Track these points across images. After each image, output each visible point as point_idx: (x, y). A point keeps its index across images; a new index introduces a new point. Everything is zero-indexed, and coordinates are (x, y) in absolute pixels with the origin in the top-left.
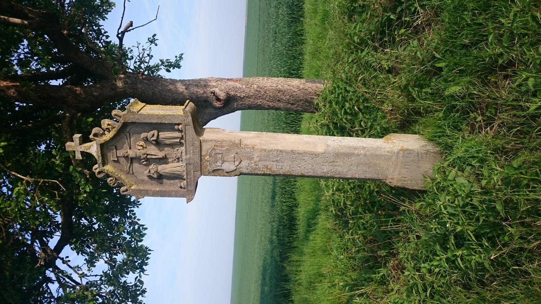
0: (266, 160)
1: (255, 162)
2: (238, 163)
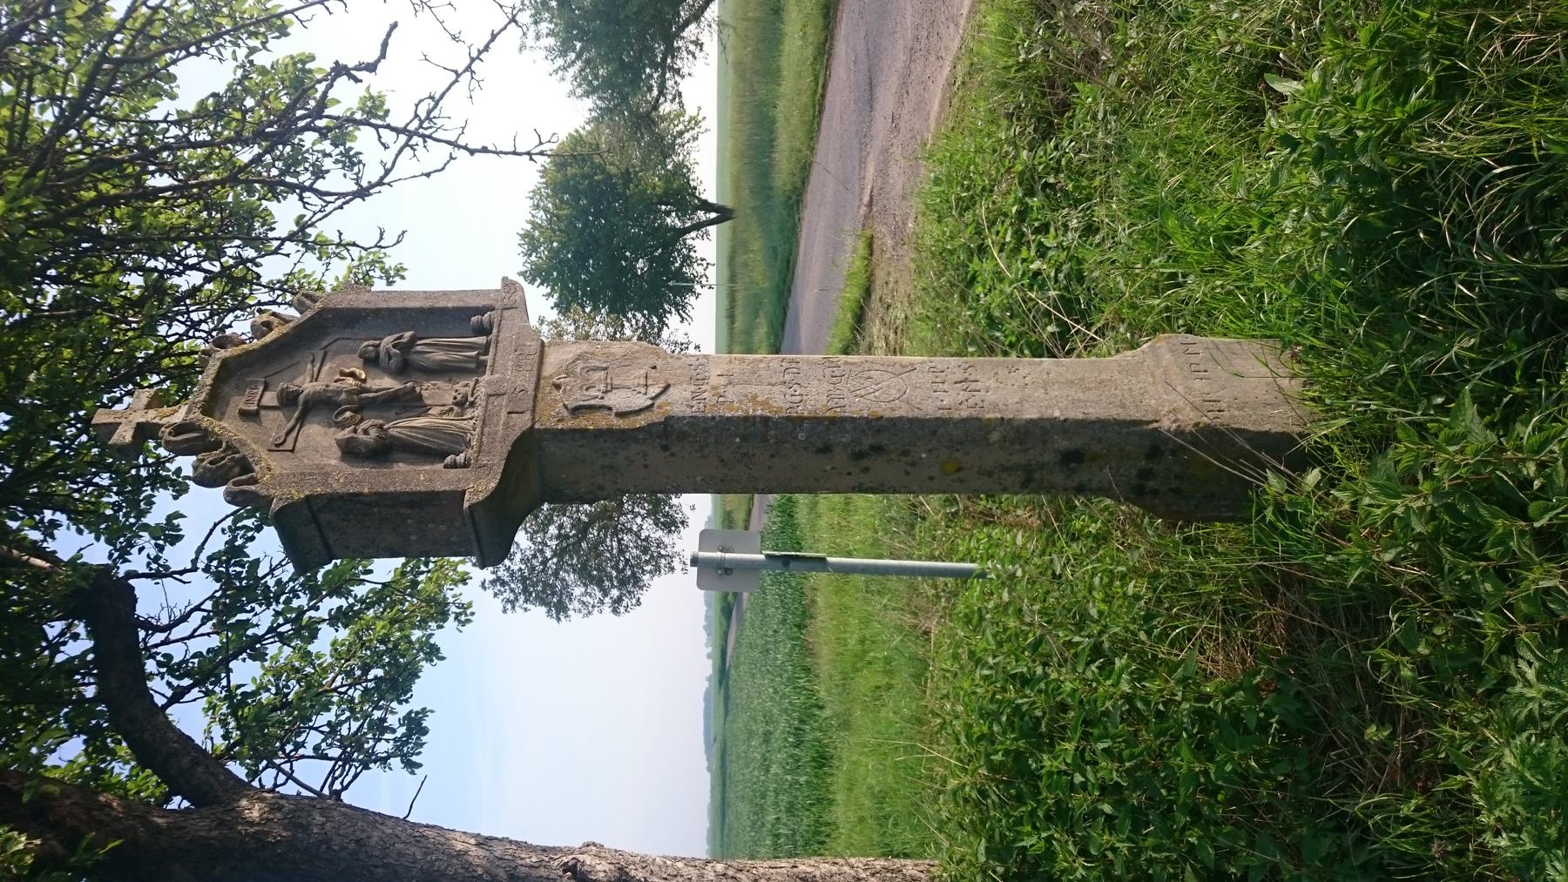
0: (747, 383)
1: (714, 388)
2: (658, 391)
